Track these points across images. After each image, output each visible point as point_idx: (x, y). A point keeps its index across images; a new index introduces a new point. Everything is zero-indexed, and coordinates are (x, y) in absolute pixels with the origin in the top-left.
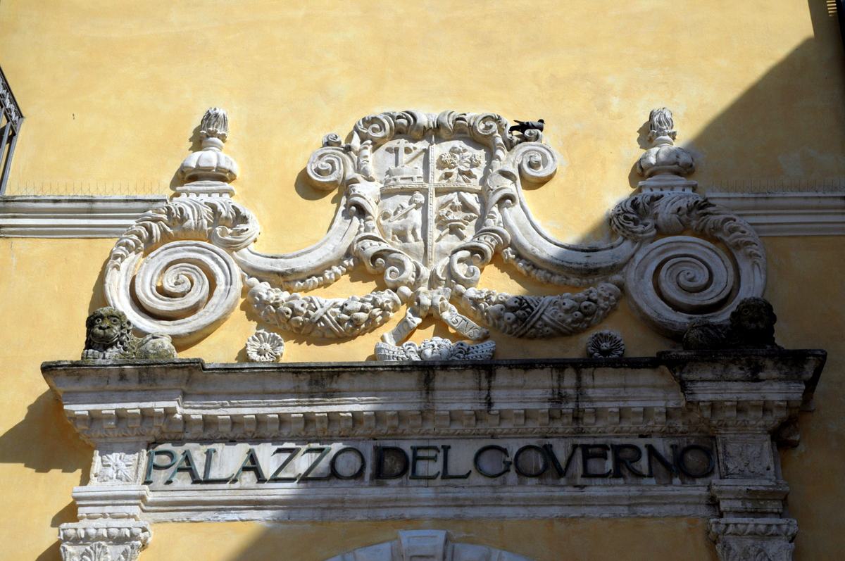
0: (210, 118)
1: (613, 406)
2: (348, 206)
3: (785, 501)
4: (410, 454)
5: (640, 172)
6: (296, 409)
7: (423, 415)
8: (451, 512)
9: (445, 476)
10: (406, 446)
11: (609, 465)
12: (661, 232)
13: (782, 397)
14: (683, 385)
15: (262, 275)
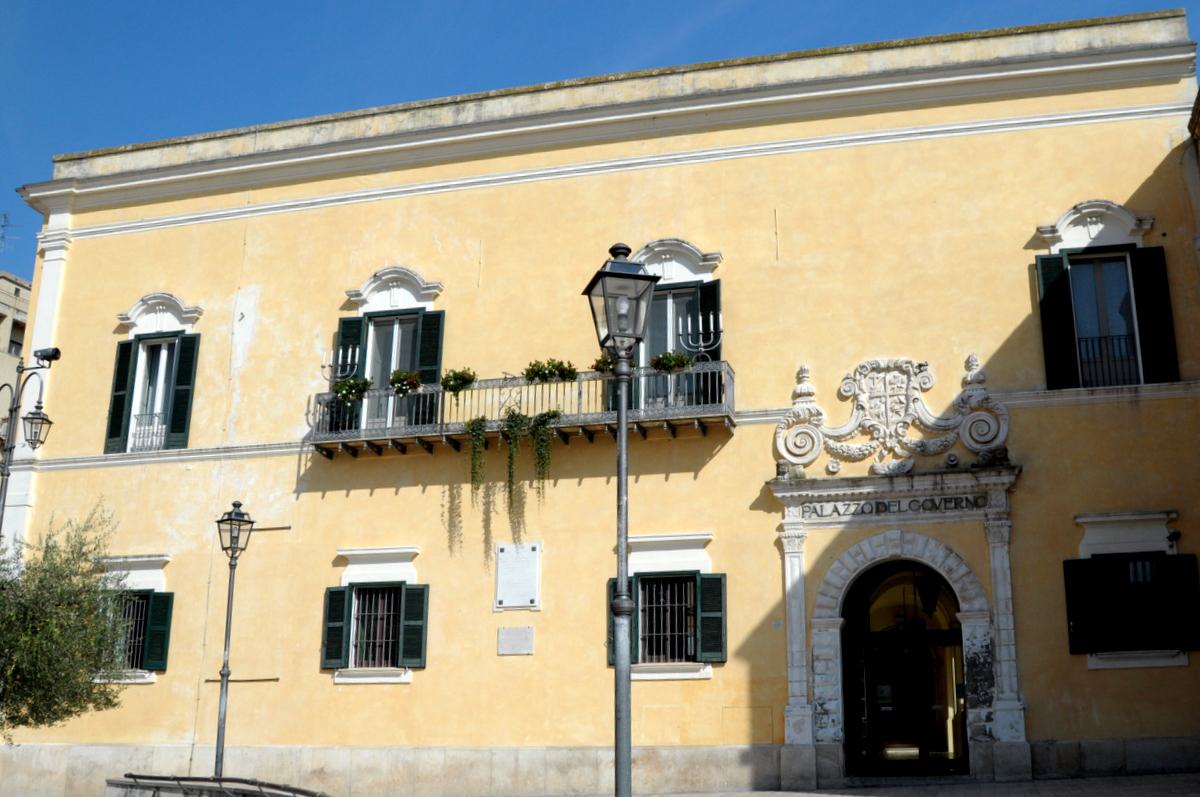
1: (954, 486)
2: (858, 405)
3: (1009, 514)
5: (965, 383)
6: (849, 491)
7: (891, 491)
8: (903, 522)
9: (899, 510)
10: (886, 501)
11: (953, 504)
12: (973, 410)
14: (977, 479)
15: (830, 437)
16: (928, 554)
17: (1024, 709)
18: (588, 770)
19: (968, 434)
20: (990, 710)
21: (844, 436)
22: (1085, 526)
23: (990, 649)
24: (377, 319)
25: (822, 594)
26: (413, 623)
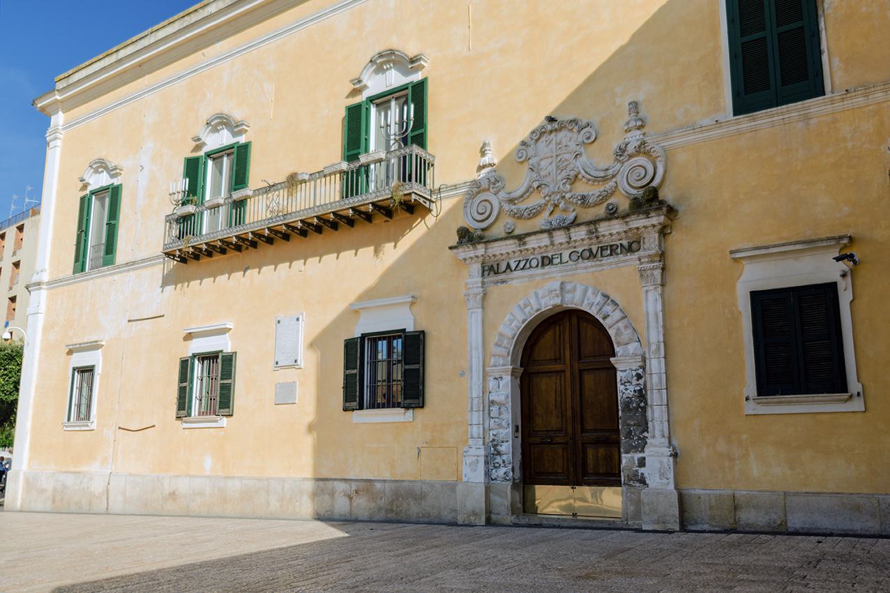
0: (485, 145)
1: (607, 233)
4: (550, 257)
9: (561, 263)
10: (550, 255)
11: (609, 252)
12: (630, 156)
13: (658, 222)
16: (586, 302)
19: (625, 181)
20: (641, 455)
21: (516, 199)
22: (744, 262)
23: (642, 395)
24: (214, 156)
25: (497, 344)
26: (225, 382)
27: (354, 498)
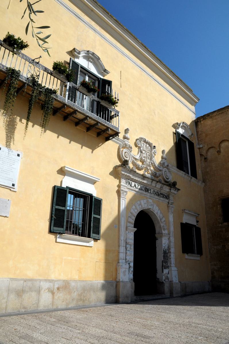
5: (162, 158)
7: (151, 185)
8: (150, 197)
14: (170, 189)
17: (177, 270)
18: (34, 294)
23: (169, 248)
27: (56, 293)
